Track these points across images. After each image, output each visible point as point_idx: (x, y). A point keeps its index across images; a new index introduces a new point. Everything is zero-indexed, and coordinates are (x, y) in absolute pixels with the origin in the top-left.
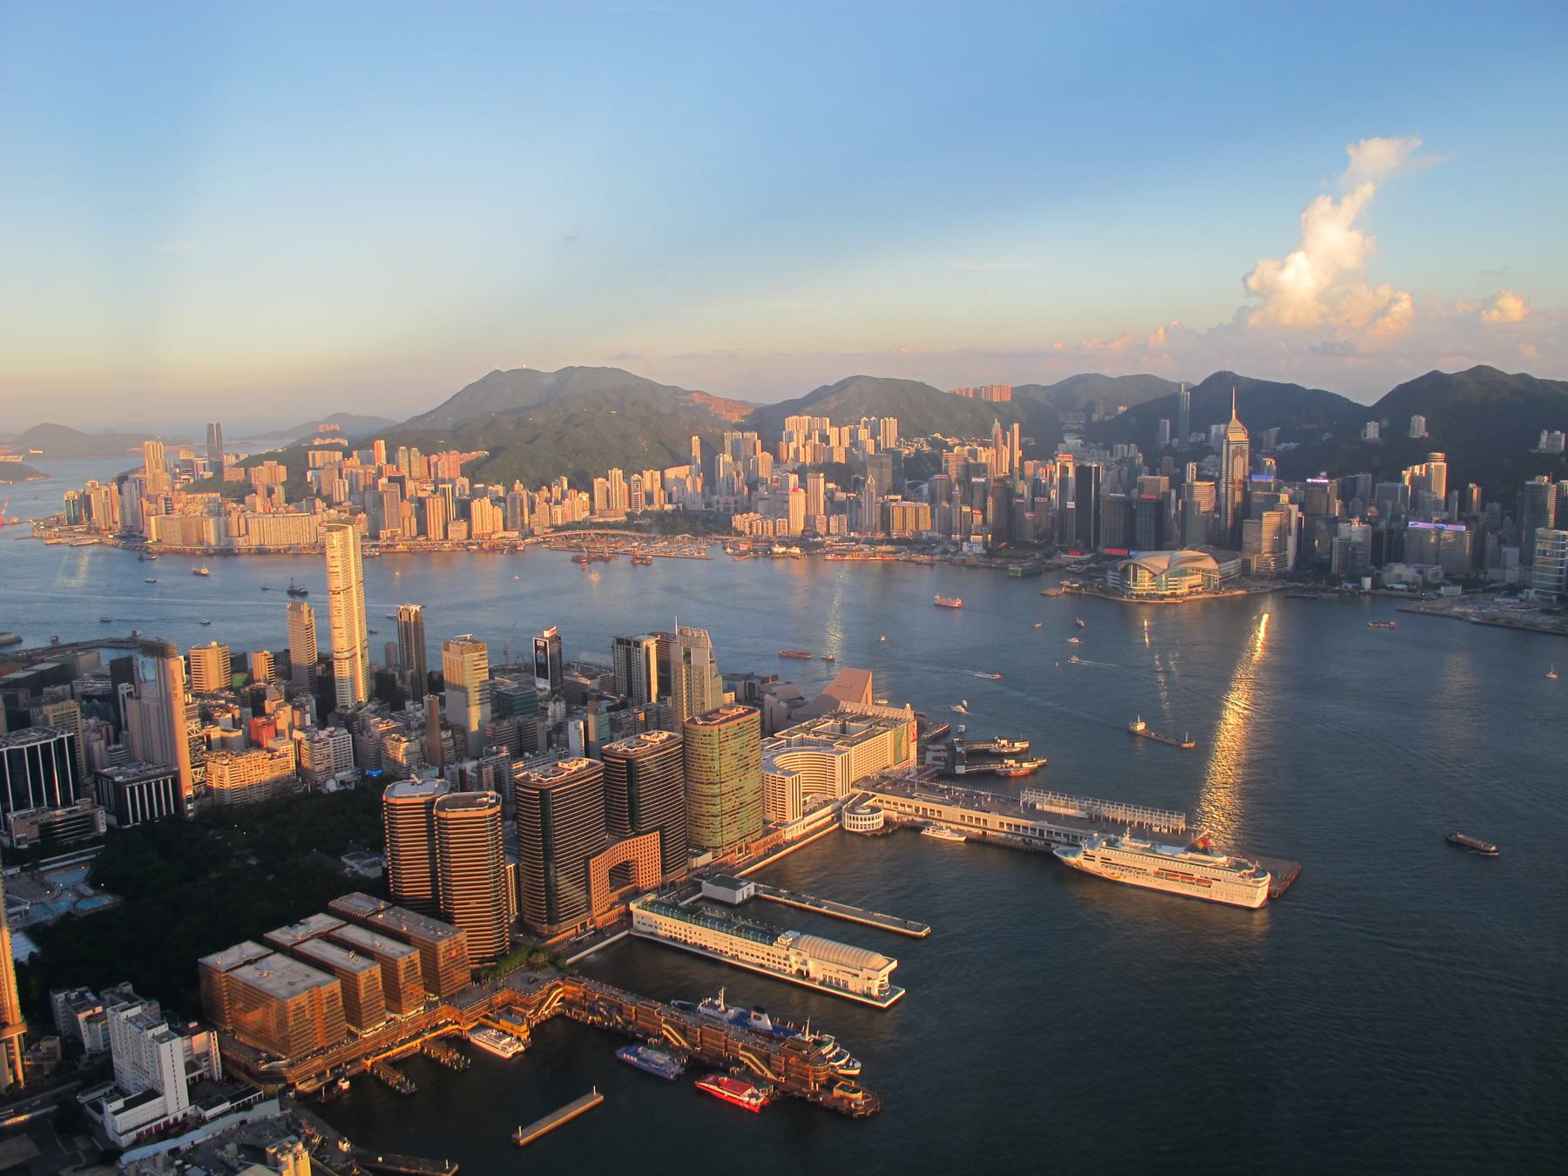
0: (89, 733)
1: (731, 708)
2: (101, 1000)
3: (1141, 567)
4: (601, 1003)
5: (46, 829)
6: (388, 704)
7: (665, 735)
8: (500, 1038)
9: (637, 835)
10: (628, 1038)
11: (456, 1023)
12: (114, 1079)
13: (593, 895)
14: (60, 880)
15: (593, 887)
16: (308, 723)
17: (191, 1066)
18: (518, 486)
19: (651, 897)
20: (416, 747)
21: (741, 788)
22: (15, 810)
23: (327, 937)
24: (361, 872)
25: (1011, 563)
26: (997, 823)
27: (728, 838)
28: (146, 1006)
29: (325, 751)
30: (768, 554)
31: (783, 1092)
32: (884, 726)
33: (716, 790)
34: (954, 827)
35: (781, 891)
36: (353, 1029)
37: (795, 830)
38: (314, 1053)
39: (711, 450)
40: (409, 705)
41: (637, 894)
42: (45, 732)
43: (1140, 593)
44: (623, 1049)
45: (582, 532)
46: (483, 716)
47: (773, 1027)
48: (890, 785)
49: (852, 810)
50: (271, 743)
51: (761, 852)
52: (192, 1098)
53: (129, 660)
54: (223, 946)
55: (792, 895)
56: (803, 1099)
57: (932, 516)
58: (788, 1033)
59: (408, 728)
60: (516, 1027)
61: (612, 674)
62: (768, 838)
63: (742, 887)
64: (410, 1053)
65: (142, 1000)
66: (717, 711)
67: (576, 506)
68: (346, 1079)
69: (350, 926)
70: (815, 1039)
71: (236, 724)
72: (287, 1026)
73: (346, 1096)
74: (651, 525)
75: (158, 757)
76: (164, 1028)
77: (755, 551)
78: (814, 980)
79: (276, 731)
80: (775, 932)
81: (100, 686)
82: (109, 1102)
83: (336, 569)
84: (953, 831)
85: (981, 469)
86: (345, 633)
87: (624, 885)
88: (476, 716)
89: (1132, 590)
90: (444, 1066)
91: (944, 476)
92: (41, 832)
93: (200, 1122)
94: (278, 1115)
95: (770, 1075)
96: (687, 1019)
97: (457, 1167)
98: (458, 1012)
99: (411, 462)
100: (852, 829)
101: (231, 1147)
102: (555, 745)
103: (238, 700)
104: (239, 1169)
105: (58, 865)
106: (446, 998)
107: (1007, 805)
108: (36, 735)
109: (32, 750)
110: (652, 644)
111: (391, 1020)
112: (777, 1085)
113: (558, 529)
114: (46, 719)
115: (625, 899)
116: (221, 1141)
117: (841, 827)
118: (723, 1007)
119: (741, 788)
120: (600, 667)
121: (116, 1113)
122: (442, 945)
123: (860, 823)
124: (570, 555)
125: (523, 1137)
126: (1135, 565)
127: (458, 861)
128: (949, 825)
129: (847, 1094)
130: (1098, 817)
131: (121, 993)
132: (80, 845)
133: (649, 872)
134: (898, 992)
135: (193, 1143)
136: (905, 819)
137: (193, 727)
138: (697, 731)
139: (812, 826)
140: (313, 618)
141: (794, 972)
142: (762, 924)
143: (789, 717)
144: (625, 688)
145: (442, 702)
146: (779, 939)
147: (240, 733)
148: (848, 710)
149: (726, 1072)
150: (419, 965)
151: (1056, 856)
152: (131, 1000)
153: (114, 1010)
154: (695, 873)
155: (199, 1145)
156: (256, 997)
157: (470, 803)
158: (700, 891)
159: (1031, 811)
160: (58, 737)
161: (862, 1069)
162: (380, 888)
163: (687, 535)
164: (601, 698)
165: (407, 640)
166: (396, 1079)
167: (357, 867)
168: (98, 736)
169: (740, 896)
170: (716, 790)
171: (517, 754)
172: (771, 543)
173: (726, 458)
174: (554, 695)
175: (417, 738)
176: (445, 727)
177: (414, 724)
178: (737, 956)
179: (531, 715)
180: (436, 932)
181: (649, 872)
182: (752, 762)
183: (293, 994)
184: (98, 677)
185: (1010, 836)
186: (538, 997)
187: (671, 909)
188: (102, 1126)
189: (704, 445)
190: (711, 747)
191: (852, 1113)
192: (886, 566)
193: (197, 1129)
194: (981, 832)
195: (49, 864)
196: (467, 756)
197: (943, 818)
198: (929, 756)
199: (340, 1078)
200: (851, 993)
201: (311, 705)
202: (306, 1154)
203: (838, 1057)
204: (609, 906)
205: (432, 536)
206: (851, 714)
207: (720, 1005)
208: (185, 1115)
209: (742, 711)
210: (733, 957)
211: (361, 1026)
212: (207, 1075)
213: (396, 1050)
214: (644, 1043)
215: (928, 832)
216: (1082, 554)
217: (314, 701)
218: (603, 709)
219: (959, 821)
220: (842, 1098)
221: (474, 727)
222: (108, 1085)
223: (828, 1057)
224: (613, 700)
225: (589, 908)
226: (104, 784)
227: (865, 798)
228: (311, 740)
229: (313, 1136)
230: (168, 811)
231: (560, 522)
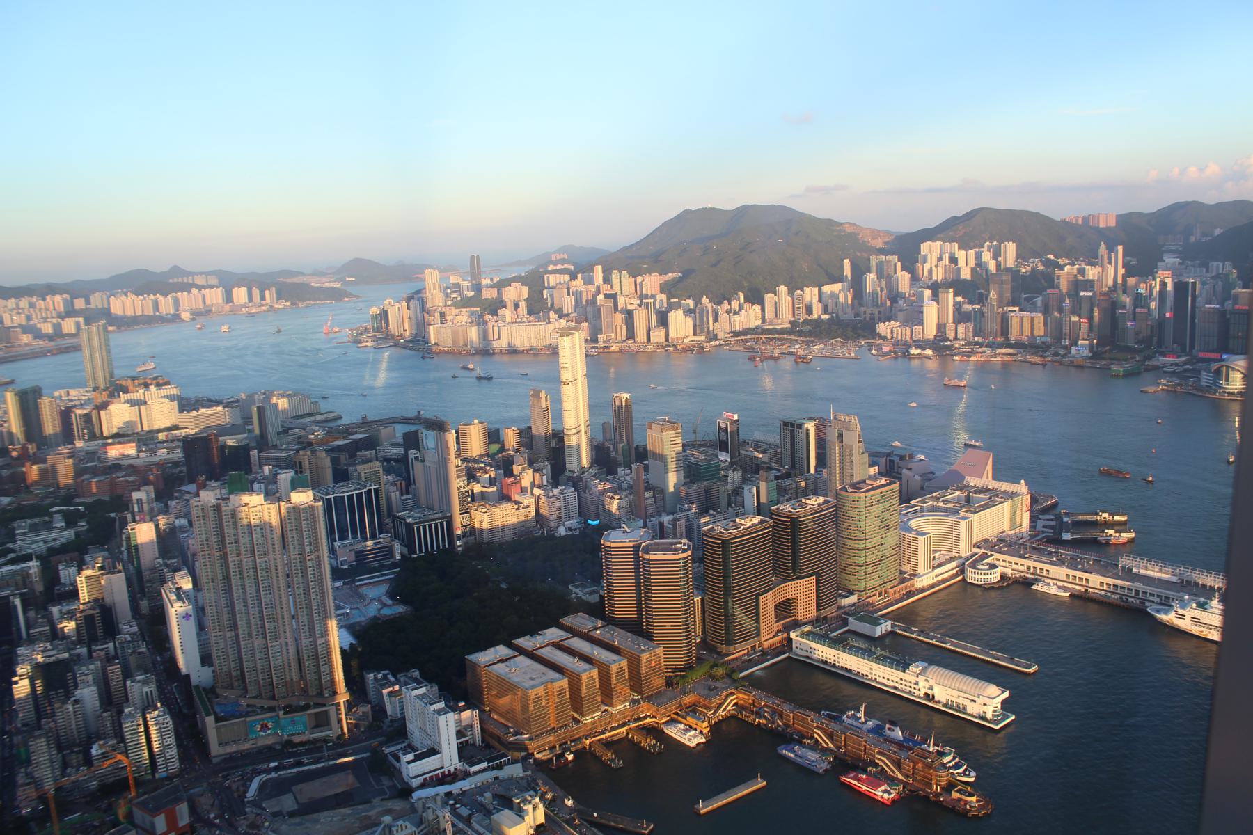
0: (388, 485)
1: (874, 478)
2: (397, 682)
3: (1233, 369)
4: (766, 709)
5: (360, 555)
6: (605, 469)
7: (821, 499)
8: (687, 731)
9: (798, 578)
10: (786, 738)
11: (654, 717)
12: (407, 739)
13: (762, 625)
14: (371, 593)
15: (762, 618)
16: (545, 483)
17: (460, 734)
18: (705, 300)
19: (808, 628)
20: (625, 503)
21: (882, 544)
22: (340, 540)
23: (558, 646)
24: (583, 597)
25: (1112, 364)
26: (1096, 582)
27: (871, 584)
28: (429, 687)
29: (557, 505)
30: (907, 356)
31: (910, 790)
32: (1002, 498)
33: (861, 545)
34: (1060, 584)
35: (913, 629)
36: (576, 716)
38: (548, 731)
39: (859, 271)
40: (621, 470)
41: (796, 625)
42: (359, 484)
43: (1231, 391)
44: (783, 747)
45: (755, 337)
46: (678, 480)
47: (904, 737)
48: (1006, 546)
49: (973, 566)
50: (517, 497)
51: (897, 596)
52: (461, 757)
53: (416, 433)
54: (483, 648)
55: (921, 632)
56: (926, 798)
57: (1045, 324)
58: (916, 743)
59: (620, 488)
60: (699, 723)
61: (779, 450)
62: (903, 586)
63: (881, 624)
64: (618, 737)
65: (426, 683)
66: (864, 482)
67: (750, 317)
68: (571, 753)
69: (576, 638)
70: (938, 750)
71: (492, 482)
72: (528, 710)
73: (570, 765)
74: (810, 331)
75: (436, 505)
76: (441, 705)
77: (895, 353)
78: (939, 702)
79: (521, 488)
80: (908, 661)
81: (396, 452)
82: (404, 754)
83: (566, 366)
84: (1060, 587)
85: (1089, 285)
86: (573, 415)
87: (786, 618)
88: (672, 479)
89: (1224, 388)
90: (643, 748)
91: (1056, 291)
92: (356, 557)
93: (466, 775)
94: (521, 775)
95: (900, 776)
96: (833, 727)
97: (652, 826)
98: (655, 708)
99: (623, 283)
100: (973, 582)
101: (488, 795)
102: (733, 505)
103: (494, 464)
104: (494, 811)
105: (368, 581)
106: (647, 698)
107: (1106, 567)
108: (353, 487)
109: (350, 497)
110: (811, 426)
111: (605, 711)
112: (905, 785)
114: (359, 473)
115: (787, 628)
116: (481, 789)
117: (964, 580)
118: (863, 720)
119: (882, 544)
120: (770, 444)
121: (409, 762)
122: (644, 657)
123: (980, 576)
124: (747, 354)
125: (703, 808)
126: (1228, 367)
127: (658, 593)
128: (1055, 582)
129: (963, 797)
130: (1189, 582)
131: (412, 677)
132: (381, 568)
133: (806, 609)
134: (1009, 717)
135: (461, 789)
136: (1018, 576)
137: (462, 484)
138: (848, 497)
139: (940, 578)
140: (548, 403)
141: (922, 695)
142: (897, 654)
143: (922, 488)
144: (789, 461)
145: (646, 469)
146: (910, 667)
147: (495, 489)
148: (972, 484)
149: (864, 771)
150: (626, 671)
151: (1150, 614)
152: (419, 682)
153: (407, 689)
154: (843, 611)
155: (465, 791)
156: (506, 687)
158: (847, 625)
159: (1128, 574)
160: (368, 488)
161: (977, 778)
162: (598, 610)
163: (839, 339)
164: (770, 468)
165: (619, 420)
166: (607, 756)
167: (581, 594)
168: (395, 488)
169: (879, 631)
170: (861, 545)
172: (907, 346)
173: (871, 278)
174: (733, 465)
175: (626, 496)
176: (648, 488)
177: (624, 486)
178: (876, 679)
179: (714, 481)
180: (640, 646)
181: (806, 609)
182: (891, 524)
183: (533, 687)
184: (392, 444)
185: (1109, 594)
186: (717, 701)
187: (824, 638)
188: (399, 771)
189: (854, 267)
190: (857, 510)
191: (967, 812)
192: (1004, 364)
193: (464, 779)
194: (1083, 590)
195: (362, 580)
196: (664, 511)
197: (1050, 576)
198: (1040, 524)
199: (567, 751)
200: (969, 715)
201: (547, 469)
202: (541, 806)
203: (957, 766)
204: (774, 633)
205: (637, 339)
206: (975, 487)
207: (860, 718)
208: (456, 769)
209: (885, 483)
210: (871, 679)
211: (582, 715)
212: (471, 741)
213: (608, 734)
214: (799, 743)
215: (1038, 587)
216: (1178, 357)
217: (549, 466)
218: (772, 478)
219: (1065, 579)
220: (959, 800)
221: (671, 489)
222: (403, 742)
223: (951, 765)
224: (779, 470)
225: (758, 634)
226: (399, 524)
227: (984, 556)
228: (546, 495)
229: (546, 793)
230: (444, 546)
231: (737, 329)
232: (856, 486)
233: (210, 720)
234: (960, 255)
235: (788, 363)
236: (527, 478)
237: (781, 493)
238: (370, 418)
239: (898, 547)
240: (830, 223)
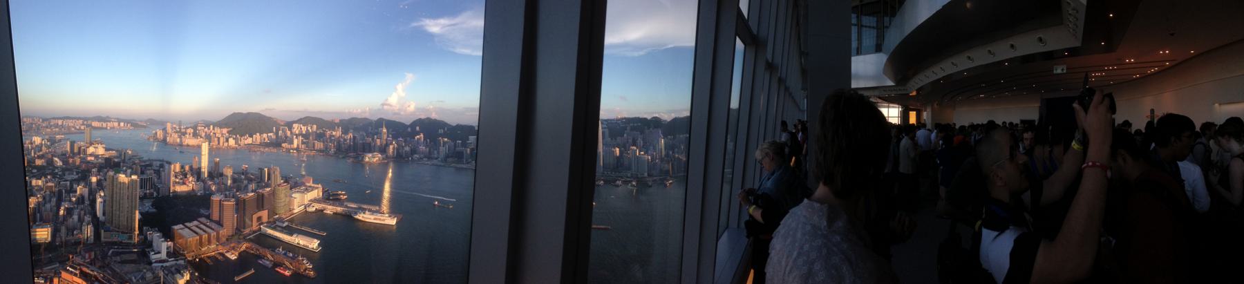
30: (290, 152)
37: (297, 210)
39: (278, 130)
67: (250, 141)
71: (181, 179)
88: (229, 182)
99: (218, 130)
110: (266, 169)
113: (246, 145)
157: (228, 201)
162: (208, 217)
171: (237, 191)
173: (280, 132)
174: (245, 179)
189: (276, 130)
221: (229, 184)
232: (279, 185)
233: (102, 231)
234: (303, 127)
235: (258, 153)
236: (191, 179)
237: (259, 187)
238: (151, 159)
239: (289, 202)
240: (270, 118)
